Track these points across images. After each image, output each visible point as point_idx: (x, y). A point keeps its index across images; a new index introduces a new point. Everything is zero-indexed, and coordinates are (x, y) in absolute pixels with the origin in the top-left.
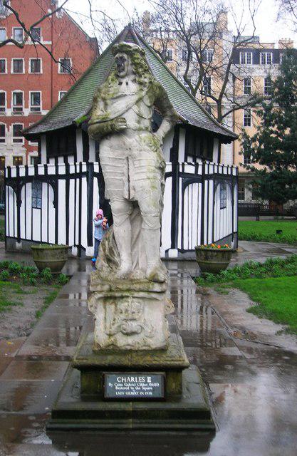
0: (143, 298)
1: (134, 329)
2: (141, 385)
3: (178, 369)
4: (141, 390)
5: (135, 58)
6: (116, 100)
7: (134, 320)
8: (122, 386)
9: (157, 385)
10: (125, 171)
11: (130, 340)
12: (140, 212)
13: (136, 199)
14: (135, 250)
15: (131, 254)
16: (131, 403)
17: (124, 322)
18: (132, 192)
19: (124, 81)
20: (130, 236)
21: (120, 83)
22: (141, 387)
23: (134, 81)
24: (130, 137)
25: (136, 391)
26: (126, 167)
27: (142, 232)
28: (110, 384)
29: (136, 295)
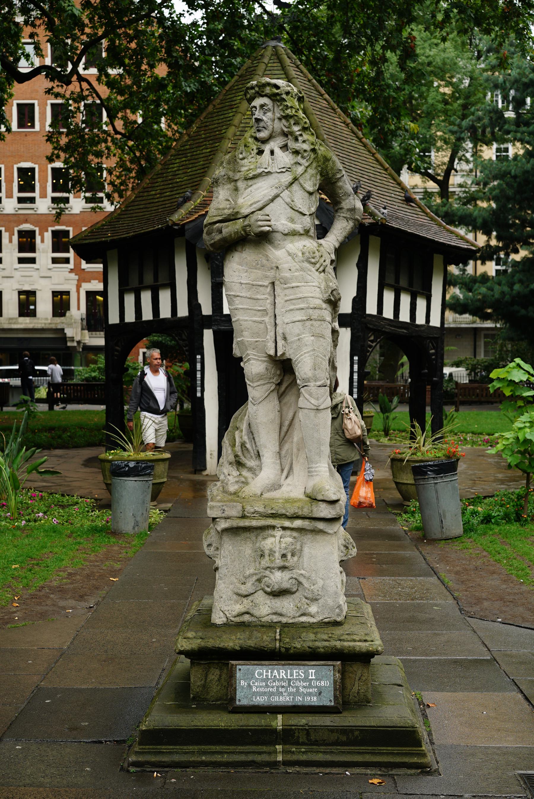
0: (300, 530)
1: (286, 585)
2: (298, 684)
3: (365, 658)
4: (298, 692)
6: (250, 183)
8: (261, 684)
10: (269, 307)
12: (295, 379)
13: (287, 356)
14: (286, 447)
15: (279, 453)
16: (280, 717)
18: (280, 343)
19: (267, 148)
20: (278, 421)
21: (260, 152)
22: (297, 687)
23: (284, 147)
24: (276, 247)
25: (290, 694)
26: (270, 300)
27: (301, 415)
29: (287, 524)
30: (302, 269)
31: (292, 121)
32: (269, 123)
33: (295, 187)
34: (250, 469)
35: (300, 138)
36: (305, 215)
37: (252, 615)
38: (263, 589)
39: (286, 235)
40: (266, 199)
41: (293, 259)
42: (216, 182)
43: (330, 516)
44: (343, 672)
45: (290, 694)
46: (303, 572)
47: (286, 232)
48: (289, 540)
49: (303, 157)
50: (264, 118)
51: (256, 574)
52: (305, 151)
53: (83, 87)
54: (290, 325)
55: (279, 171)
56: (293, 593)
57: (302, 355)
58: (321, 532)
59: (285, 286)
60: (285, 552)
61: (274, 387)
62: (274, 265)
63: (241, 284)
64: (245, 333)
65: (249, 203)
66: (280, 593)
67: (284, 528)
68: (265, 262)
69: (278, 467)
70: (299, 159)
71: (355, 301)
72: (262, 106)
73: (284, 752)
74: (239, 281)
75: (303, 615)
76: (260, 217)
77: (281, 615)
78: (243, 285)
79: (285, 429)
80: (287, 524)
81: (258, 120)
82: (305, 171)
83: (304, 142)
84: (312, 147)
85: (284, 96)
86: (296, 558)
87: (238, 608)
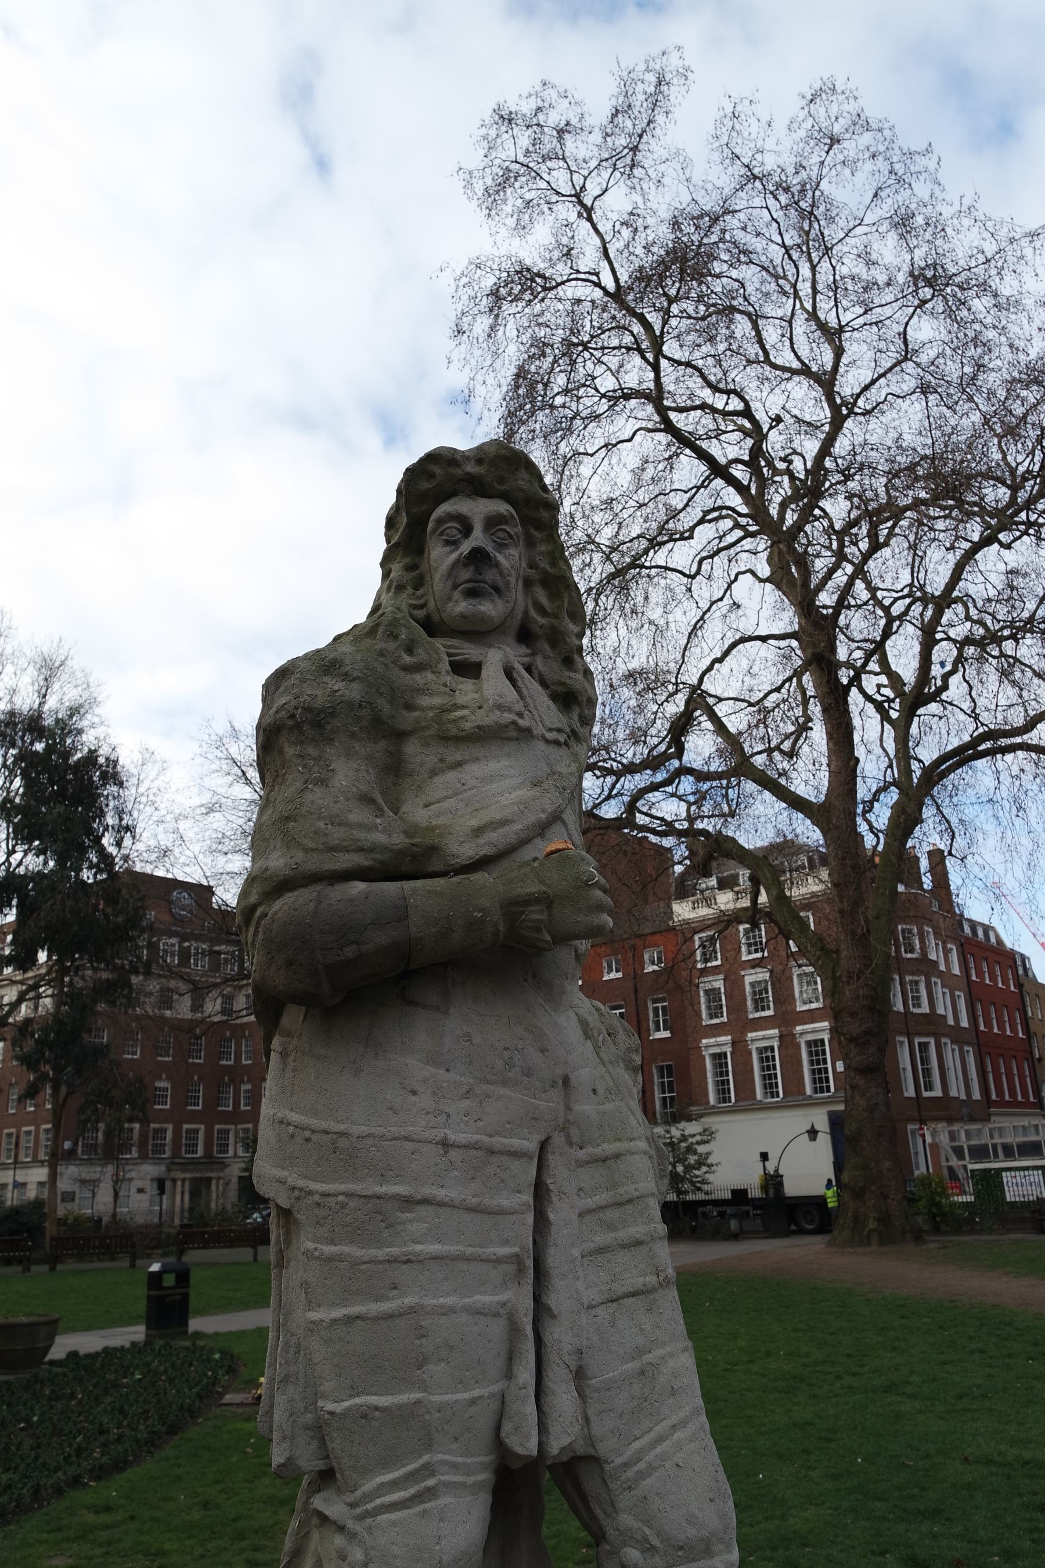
6: (454, 754)
13: (581, 1450)
18: (563, 1397)
40: (532, 818)
42: (318, 725)
50: (500, 558)
54: (601, 1311)
55: (550, 736)
57: (660, 1439)
59: (581, 1154)
63: (446, 1145)
65: (474, 823)
74: (439, 1134)
78: (453, 1154)
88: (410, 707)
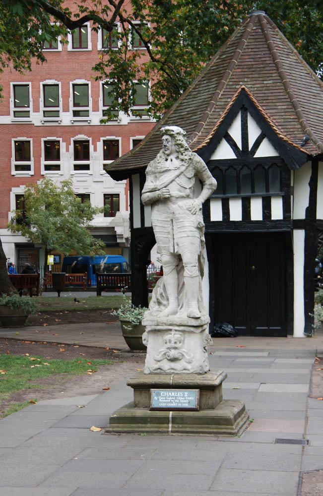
0: (183, 331)
1: (177, 356)
2: (179, 398)
4: (180, 402)
5: (177, 140)
6: (162, 174)
7: (176, 348)
8: (162, 398)
9: (192, 398)
10: (170, 230)
11: (173, 365)
14: (181, 295)
15: (178, 298)
16: (171, 412)
17: (168, 351)
18: (176, 247)
19: (169, 158)
20: (176, 283)
21: (167, 160)
23: (177, 158)
28: (156, 398)
30: (185, 213)
31: (180, 146)
32: (170, 147)
33: (182, 176)
34: (165, 305)
35: (184, 154)
36: (186, 188)
37: (161, 370)
38: (166, 358)
39: (177, 198)
40: (168, 182)
41: (181, 208)
43: (195, 325)
44: (201, 395)
45: (177, 402)
46: (184, 350)
47: (177, 196)
48: (178, 336)
49: (185, 162)
50: (168, 145)
51: (163, 351)
52: (186, 160)
53: (125, 27)
56: (180, 360)
58: (192, 332)
60: (176, 341)
61: (174, 267)
62: (172, 212)
64: (160, 243)
65: (161, 183)
66: (174, 360)
67: (176, 331)
68: (168, 210)
69: (177, 304)
70: (183, 163)
71: (307, 210)
72: (166, 140)
73: (172, 427)
75: (185, 369)
76: (165, 191)
77: (175, 369)
79: (180, 286)
80: (177, 328)
81: (165, 146)
82: (187, 169)
83: (186, 155)
84: (190, 157)
85: (175, 135)
86: (181, 344)
87: (157, 366)
88: (157, 169)
